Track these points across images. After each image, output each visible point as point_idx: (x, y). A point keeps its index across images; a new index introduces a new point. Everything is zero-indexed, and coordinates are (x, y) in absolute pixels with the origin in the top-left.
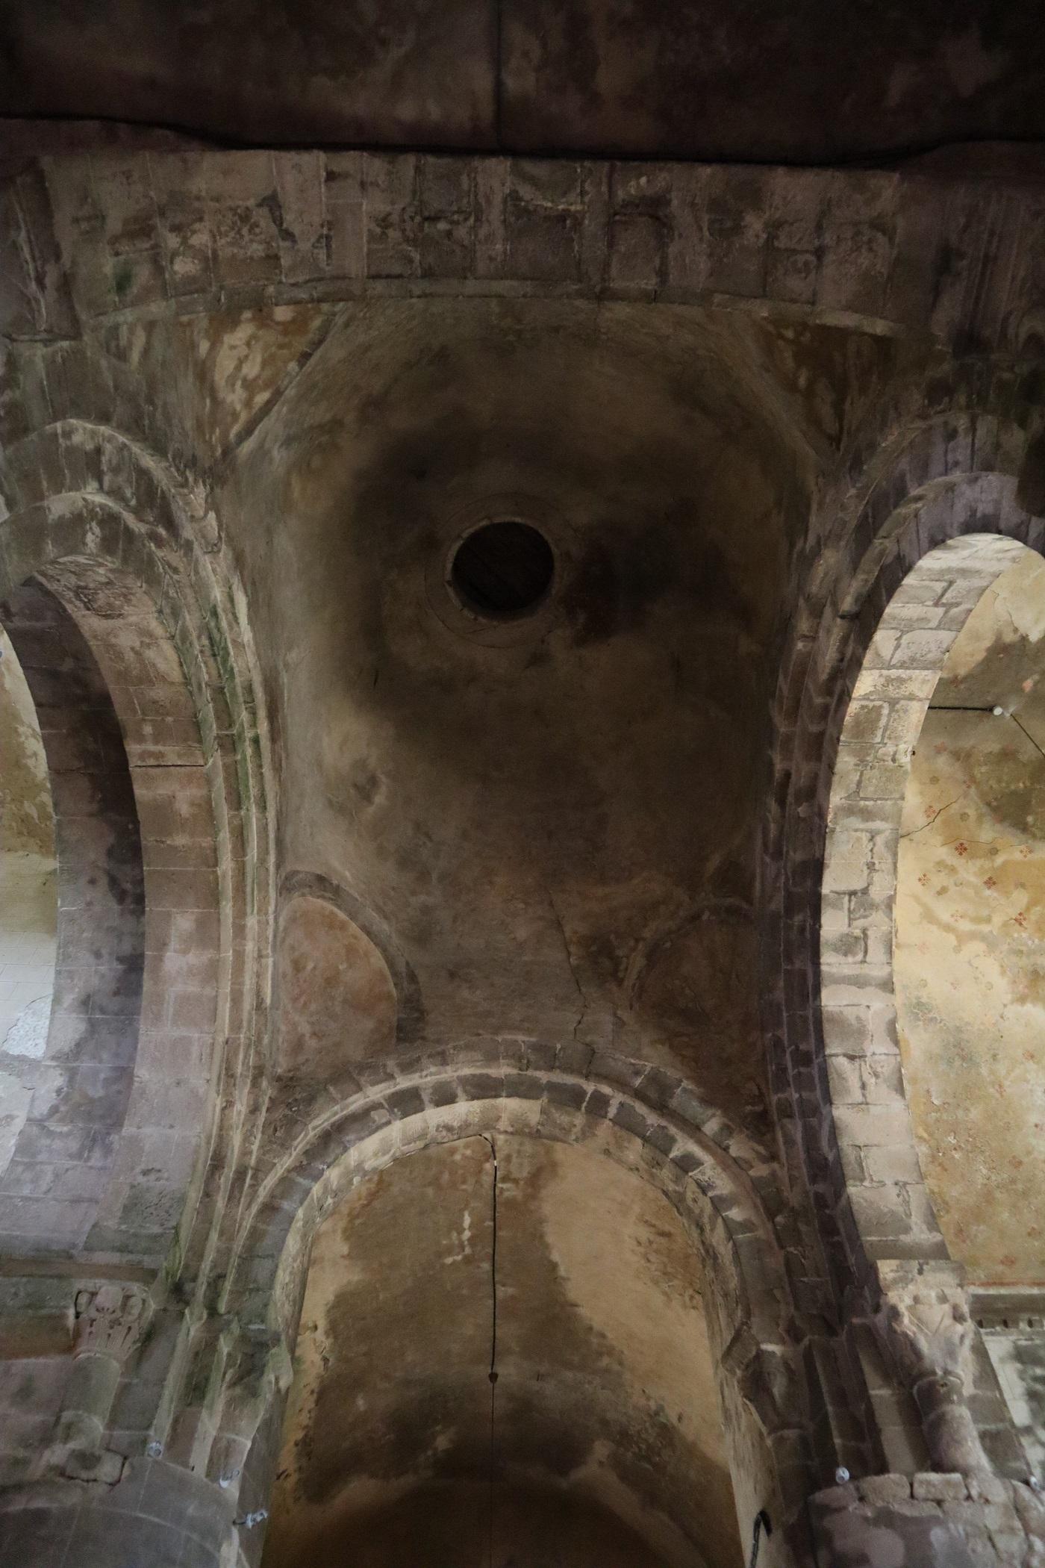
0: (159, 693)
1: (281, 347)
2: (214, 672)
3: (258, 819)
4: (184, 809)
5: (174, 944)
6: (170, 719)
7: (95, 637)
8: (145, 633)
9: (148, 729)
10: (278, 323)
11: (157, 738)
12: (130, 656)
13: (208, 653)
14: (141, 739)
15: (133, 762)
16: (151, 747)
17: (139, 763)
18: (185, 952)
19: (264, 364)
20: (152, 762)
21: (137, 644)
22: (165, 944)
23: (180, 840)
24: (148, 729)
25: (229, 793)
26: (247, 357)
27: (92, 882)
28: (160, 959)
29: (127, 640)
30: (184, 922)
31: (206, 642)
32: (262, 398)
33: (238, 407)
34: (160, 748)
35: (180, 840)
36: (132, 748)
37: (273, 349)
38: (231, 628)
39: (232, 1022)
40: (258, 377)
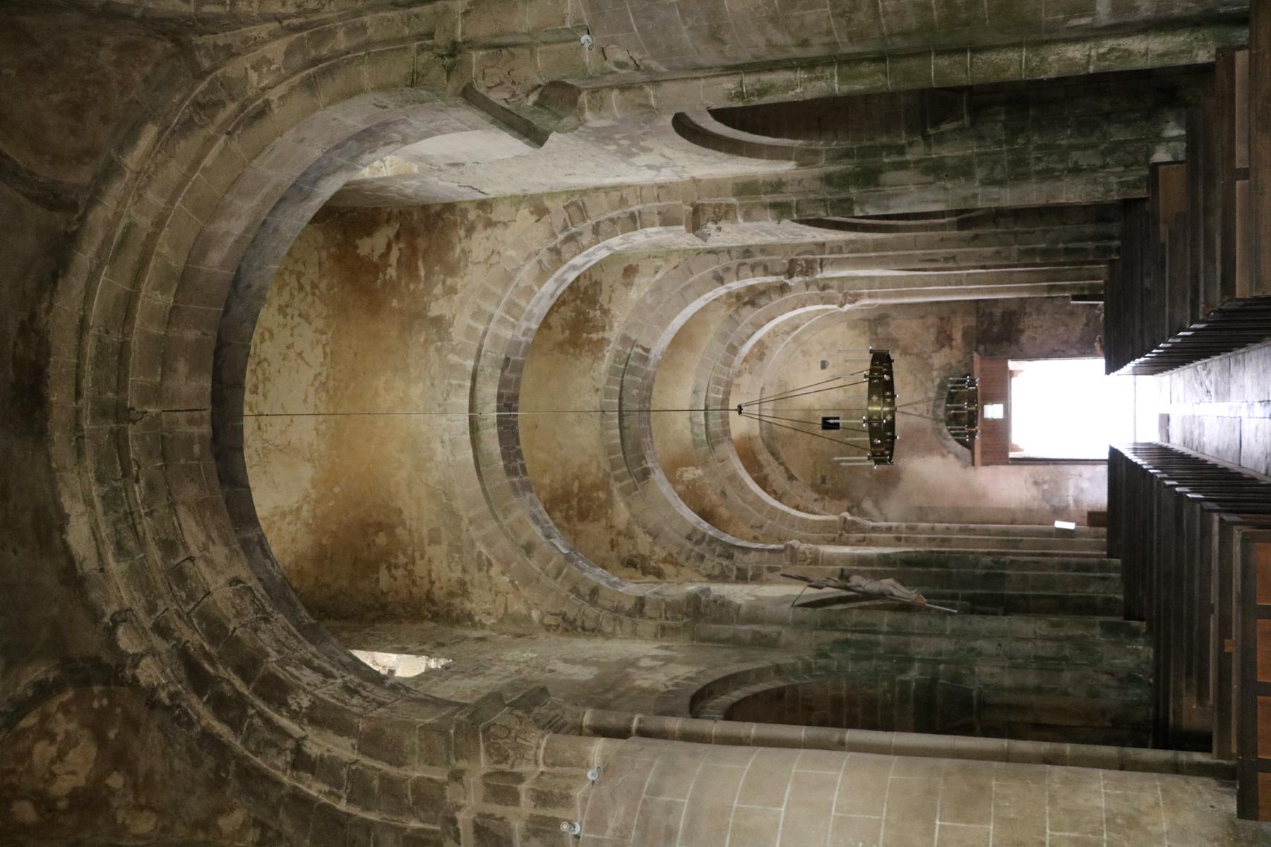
0: (191, 491)
1: (13, 771)
2: (131, 494)
3: (91, 309)
4: (182, 367)
5: (230, 241)
6: (182, 462)
7: (238, 555)
8: (210, 563)
9: (196, 449)
10: (23, 798)
11: (189, 440)
12: (215, 535)
13: (136, 515)
14: (202, 437)
15: (207, 414)
16: (195, 430)
17: (204, 413)
18: (228, 233)
19: (29, 753)
20: (196, 414)
21: (211, 548)
22: (236, 241)
23: (191, 335)
24: (196, 449)
25: (127, 359)
26: (53, 762)
27: (249, 286)
28: (247, 230)
29: (219, 552)
30: (215, 257)
31: (139, 528)
32: (30, 721)
33: (60, 716)
34: (190, 430)
35: (191, 335)
36: (206, 429)
37: (20, 768)
38: (97, 525)
39: (212, 146)
40: (36, 741)
